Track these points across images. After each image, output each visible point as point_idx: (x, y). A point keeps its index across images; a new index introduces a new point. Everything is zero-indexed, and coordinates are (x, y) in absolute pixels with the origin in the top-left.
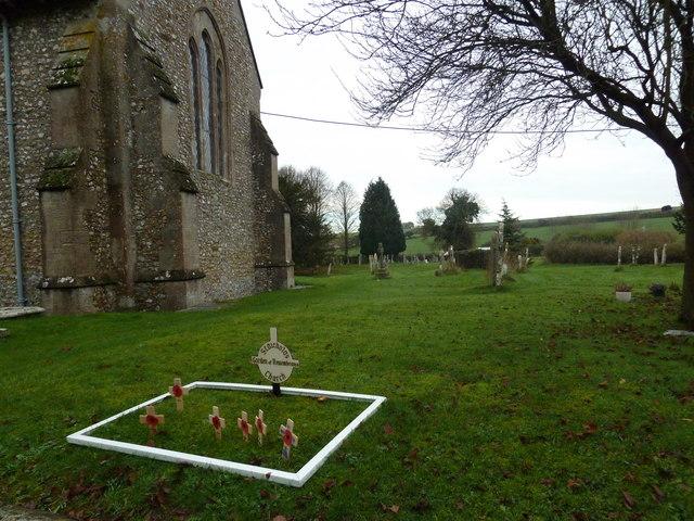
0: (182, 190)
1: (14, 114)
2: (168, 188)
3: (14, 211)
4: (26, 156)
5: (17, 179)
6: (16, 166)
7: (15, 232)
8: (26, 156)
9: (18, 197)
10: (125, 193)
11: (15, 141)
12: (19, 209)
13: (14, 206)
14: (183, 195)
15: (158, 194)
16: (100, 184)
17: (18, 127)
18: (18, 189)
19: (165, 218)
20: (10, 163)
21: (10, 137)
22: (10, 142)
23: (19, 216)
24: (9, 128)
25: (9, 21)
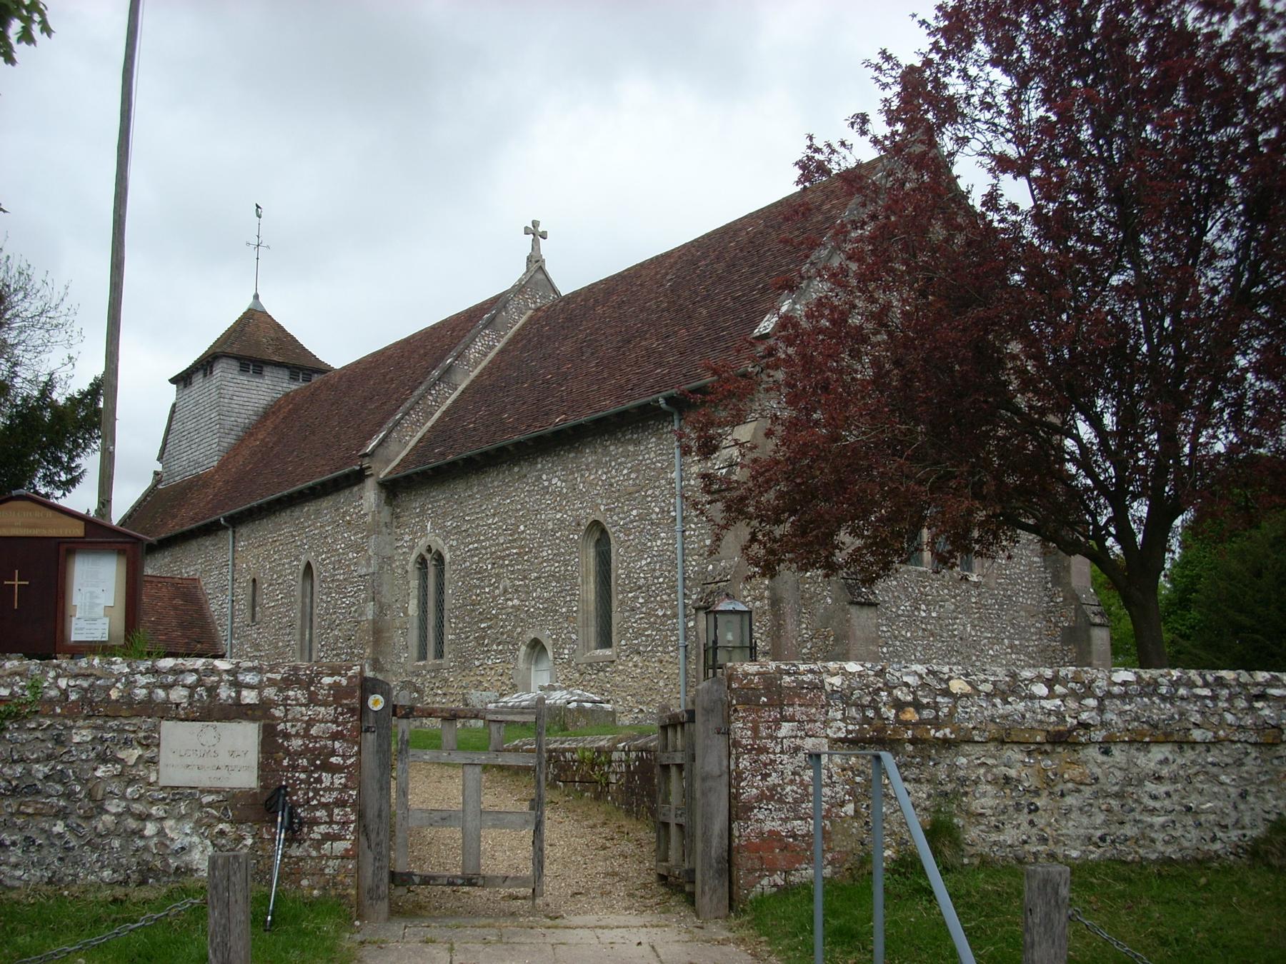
0: (852, 603)
1: (684, 518)
2: (835, 600)
3: (680, 632)
4: (694, 566)
5: (685, 594)
6: (684, 579)
7: (681, 656)
8: (694, 566)
9: (686, 616)
10: (787, 608)
11: (684, 549)
12: (686, 629)
13: (680, 627)
14: (854, 610)
15: (825, 609)
16: (761, 598)
17: (687, 533)
18: (685, 606)
19: (832, 639)
20: (679, 576)
21: (678, 545)
22: (679, 552)
23: (686, 638)
24: (679, 535)
25: (680, 413)
